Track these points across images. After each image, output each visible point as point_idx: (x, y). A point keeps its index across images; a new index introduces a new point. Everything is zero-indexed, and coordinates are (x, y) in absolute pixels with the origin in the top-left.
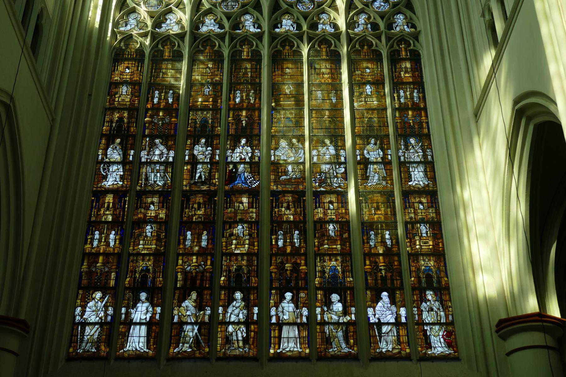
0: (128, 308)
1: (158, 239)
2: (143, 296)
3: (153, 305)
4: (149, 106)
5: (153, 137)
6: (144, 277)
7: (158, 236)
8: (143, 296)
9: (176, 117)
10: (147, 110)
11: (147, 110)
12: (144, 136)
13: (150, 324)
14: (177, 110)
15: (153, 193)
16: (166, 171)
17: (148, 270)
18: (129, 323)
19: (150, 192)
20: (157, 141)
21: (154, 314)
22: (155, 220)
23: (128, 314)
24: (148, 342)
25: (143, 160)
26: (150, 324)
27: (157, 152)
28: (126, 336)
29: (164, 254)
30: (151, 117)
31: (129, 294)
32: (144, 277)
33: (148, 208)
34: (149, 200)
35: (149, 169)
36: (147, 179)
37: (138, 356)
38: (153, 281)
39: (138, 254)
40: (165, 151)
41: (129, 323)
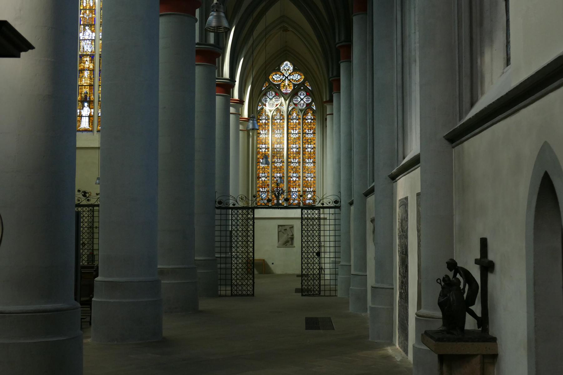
0: (80, 109)
1: (91, 79)
2: (86, 104)
3: (90, 109)
4: (82, 8)
5: (85, 25)
6: (86, 96)
7: (90, 77)
8: (86, 104)
9: (95, 14)
10: (81, 10)
11: (81, 10)
12: (81, 25)
13: (90, 116)
14: (95, 10)
15: (87, 55)
16: (91, 44)
17: (87, 93)
18: (81, 116)
19: (85, 55)
20: (87, 28)
21: (91, 112)
22: (88, 69)
23: (80, 112)
24: (89, 124)
25: (81, 38)
26: (90, 116)
27: (87, 33)
28: (80, 121)
29: (93, 85)
30: (83, 14)
31: (80, 104)
32: (86, 96)
33: (85, 63)
34: (85, 59)
35: (84, 43)
36: (83, 49)
37: (86, 130)
38: (90, 98)
39: (82, 85)
40: (91, 33)
41: (81, 116)
